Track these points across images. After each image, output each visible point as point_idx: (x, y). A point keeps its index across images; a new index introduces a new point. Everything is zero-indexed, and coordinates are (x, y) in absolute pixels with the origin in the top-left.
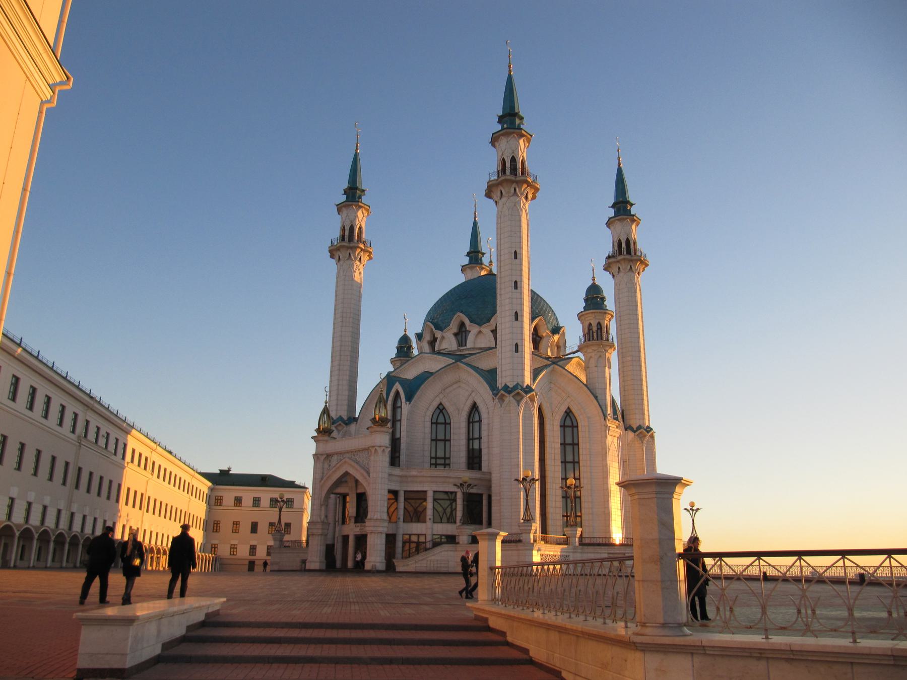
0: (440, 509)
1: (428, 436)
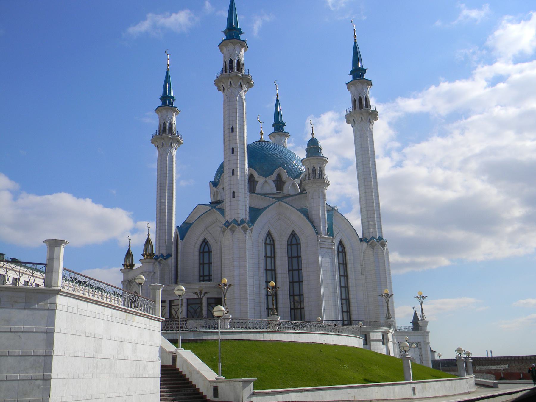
0: (192, 311)
1: (197, 261)
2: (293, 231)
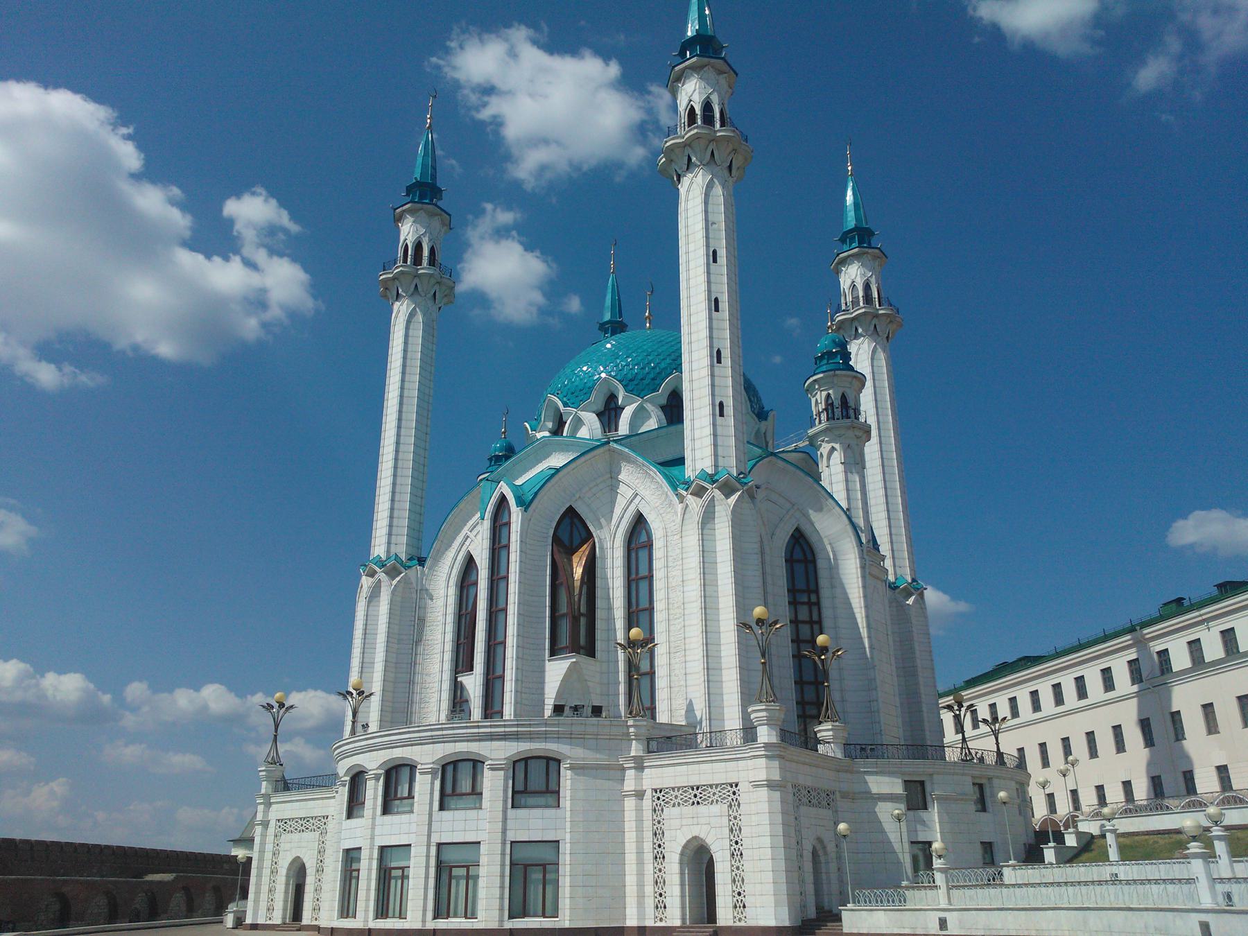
2: (797, 530)
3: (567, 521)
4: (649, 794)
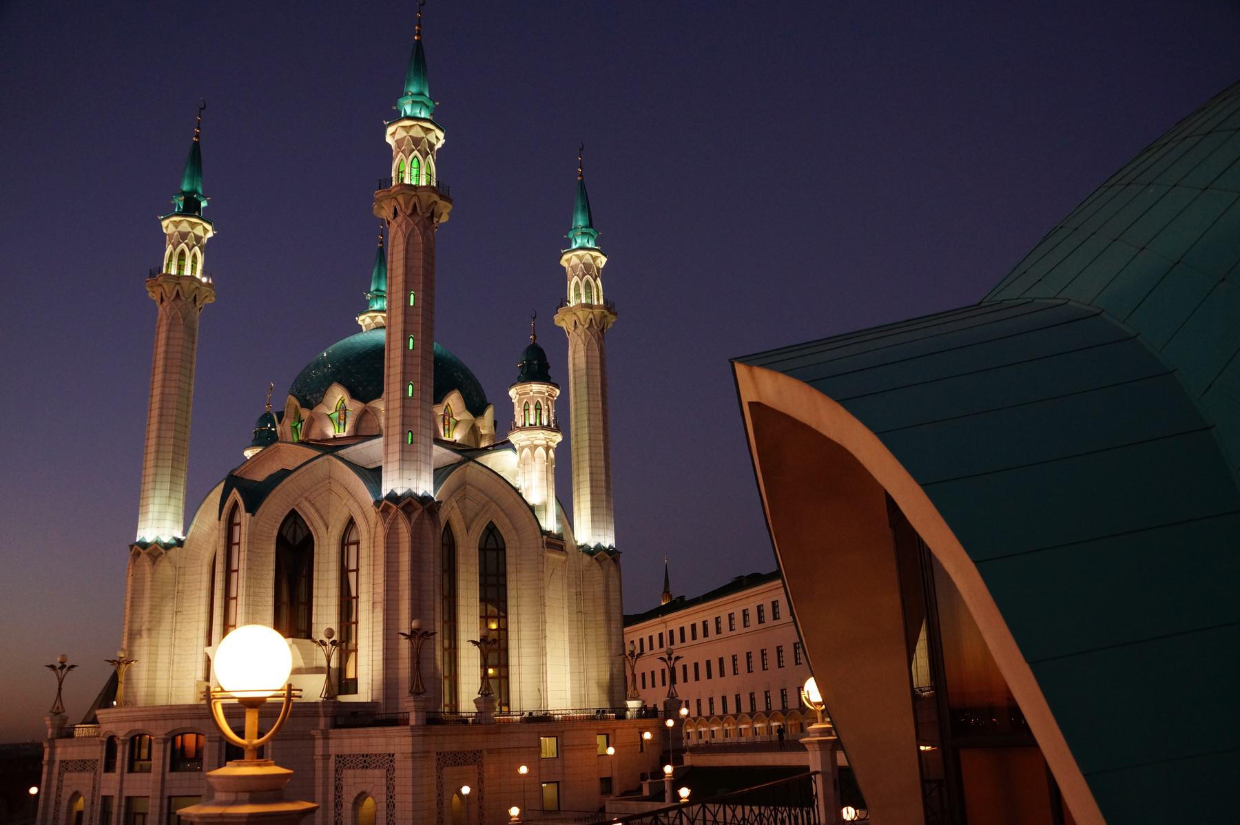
3: (292, 520)
4: (333, 757)
